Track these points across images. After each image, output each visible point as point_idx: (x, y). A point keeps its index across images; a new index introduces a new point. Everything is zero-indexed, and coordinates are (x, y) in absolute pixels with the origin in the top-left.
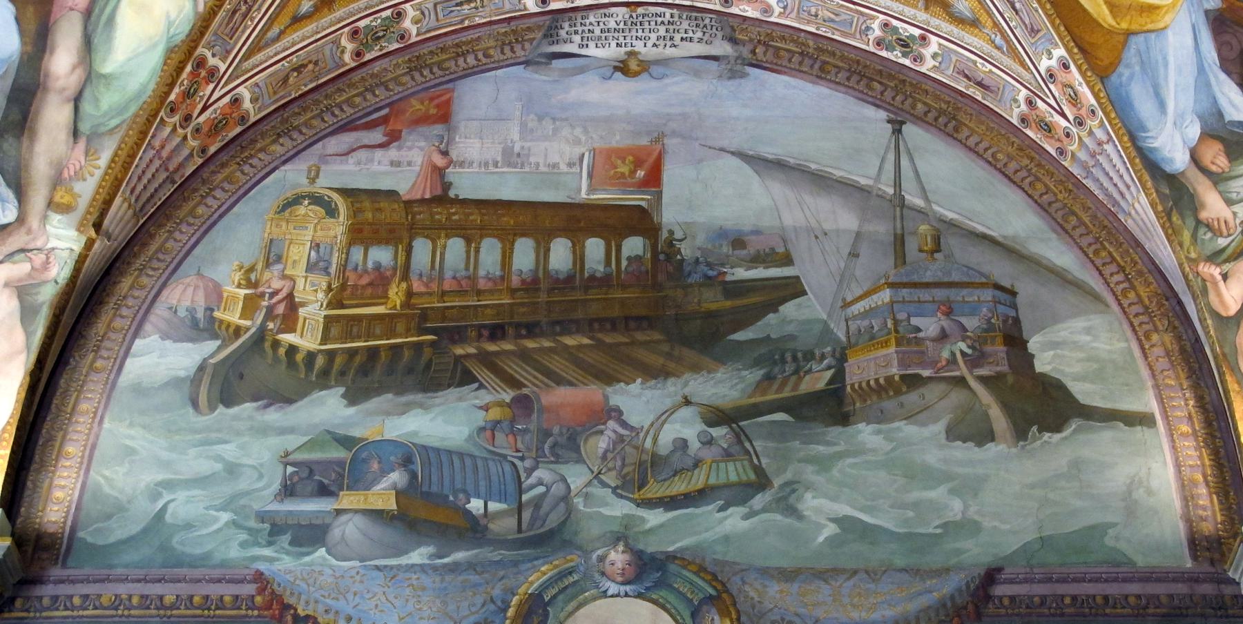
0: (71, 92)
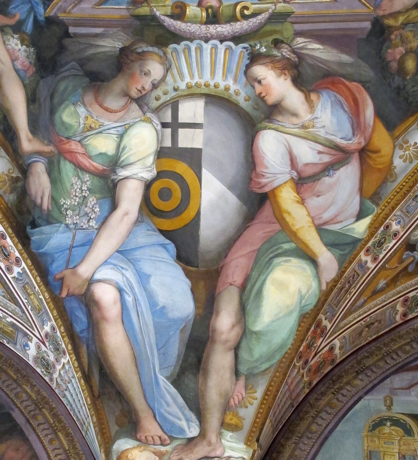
0: (232, 344)
